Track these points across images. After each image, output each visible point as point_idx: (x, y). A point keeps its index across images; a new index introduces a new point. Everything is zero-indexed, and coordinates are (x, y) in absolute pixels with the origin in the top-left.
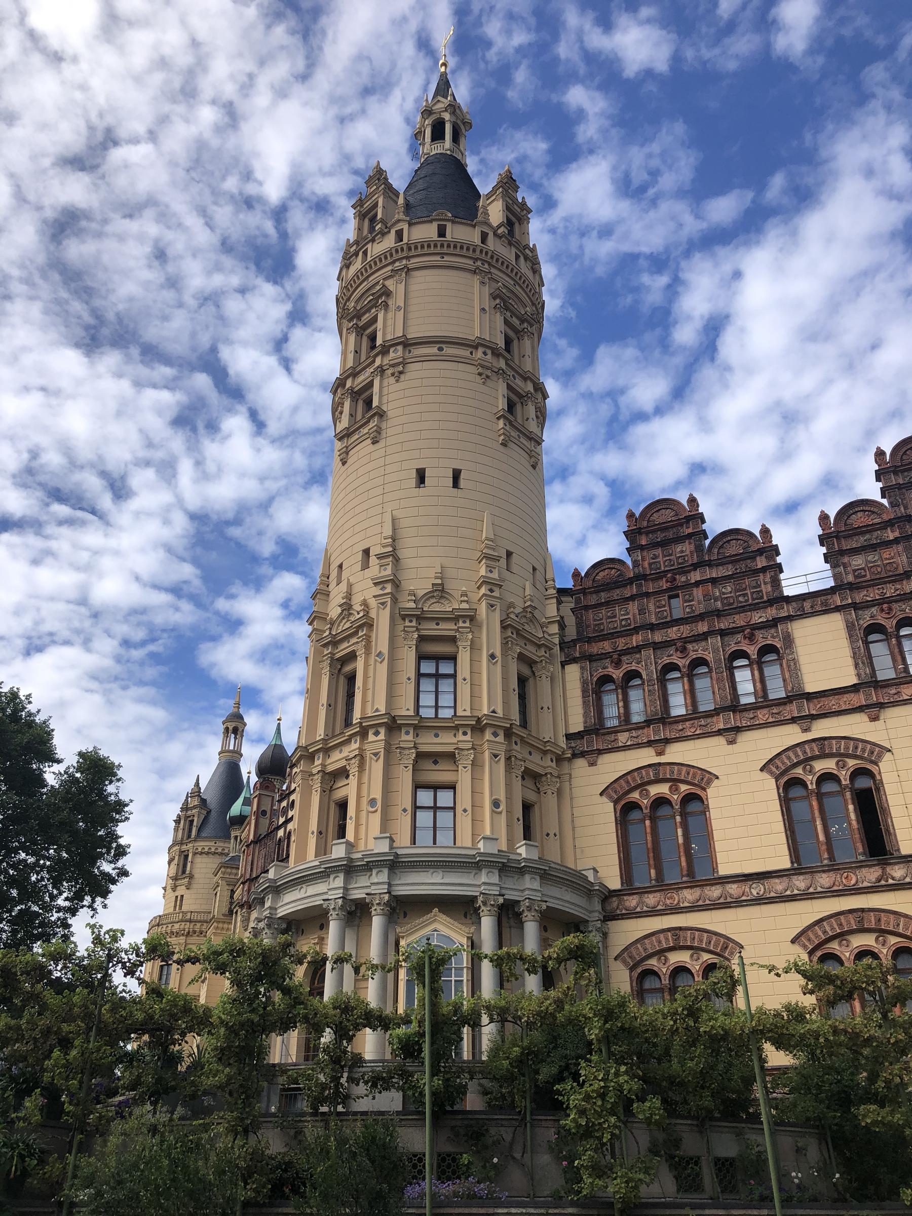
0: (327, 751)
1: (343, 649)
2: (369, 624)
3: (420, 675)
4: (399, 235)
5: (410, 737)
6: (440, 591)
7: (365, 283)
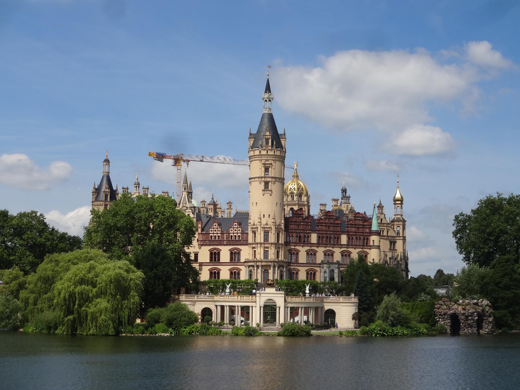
0: (253, 244)
1: (254, 230)
2: (257, 228)
3: (264, 235)
4: (260, 151)
5: (263, 245)
6: (267, 224)
7: (254, 159)
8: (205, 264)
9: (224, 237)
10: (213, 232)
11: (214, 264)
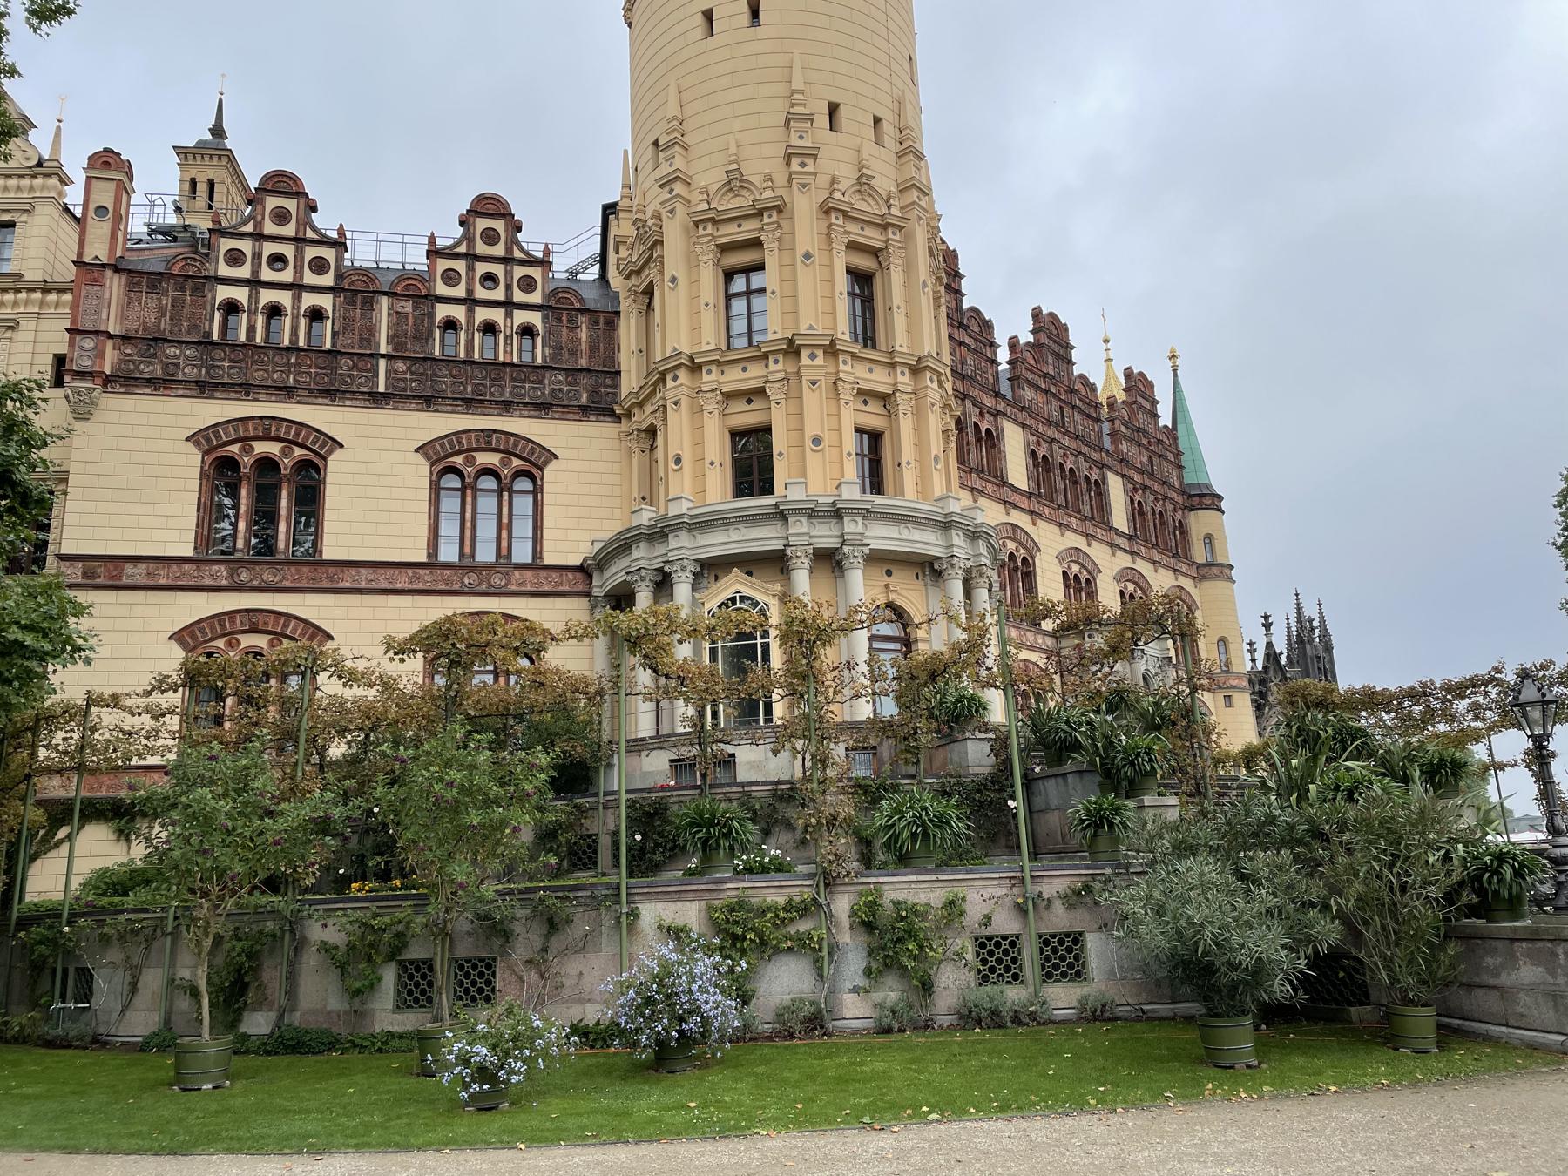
1: (730, 233)
8: (132, 573)
9: (372, 331)
10: (255, 272)
11: (244, 576)
